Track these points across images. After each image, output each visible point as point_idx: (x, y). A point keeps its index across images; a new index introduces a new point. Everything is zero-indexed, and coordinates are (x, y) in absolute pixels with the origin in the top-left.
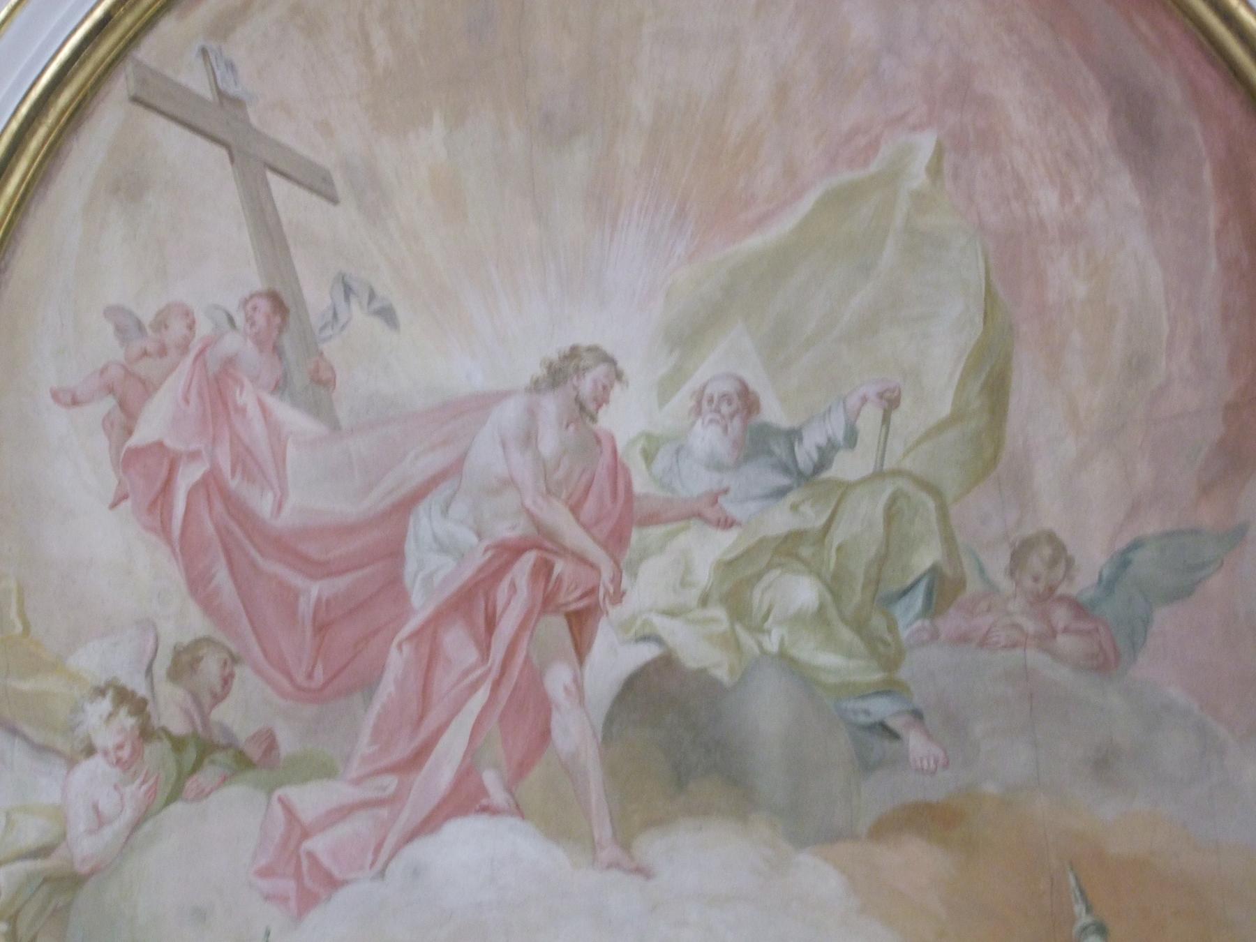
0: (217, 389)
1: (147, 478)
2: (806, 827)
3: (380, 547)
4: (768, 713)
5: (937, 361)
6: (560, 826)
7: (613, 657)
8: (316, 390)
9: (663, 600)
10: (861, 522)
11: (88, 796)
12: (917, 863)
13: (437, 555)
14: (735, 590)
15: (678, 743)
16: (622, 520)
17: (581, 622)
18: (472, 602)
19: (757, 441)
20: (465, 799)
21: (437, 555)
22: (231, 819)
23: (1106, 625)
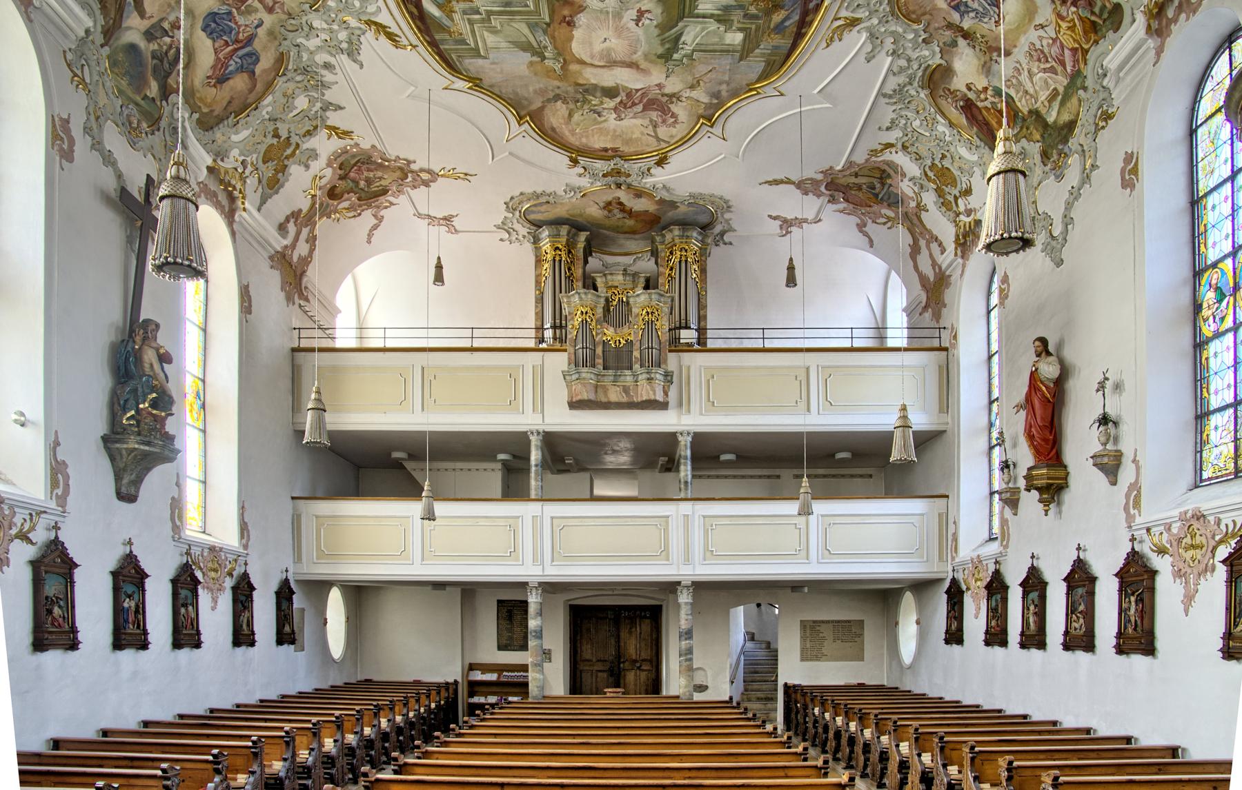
0: (664, 121)
1: (674, 115)
2: (595, 86)
3: (644, 109)
4: (598, 94)
5: (576, 117)
6: (625, 88)
7: (618, 100)
8: (651, 121)
9: (611, 104)
10: (586, 107)
11: (687, 93)
12: (581, 82)
13: (640, 108)
14: (602, 103)
15: (611, 92)
16: (615, 109)
17: (621, 102)
18: (634, 104)
19: (599, 114)
20: (637, 90)
21: (640, 108)
22: (667, 90)
23: (557, 98)
